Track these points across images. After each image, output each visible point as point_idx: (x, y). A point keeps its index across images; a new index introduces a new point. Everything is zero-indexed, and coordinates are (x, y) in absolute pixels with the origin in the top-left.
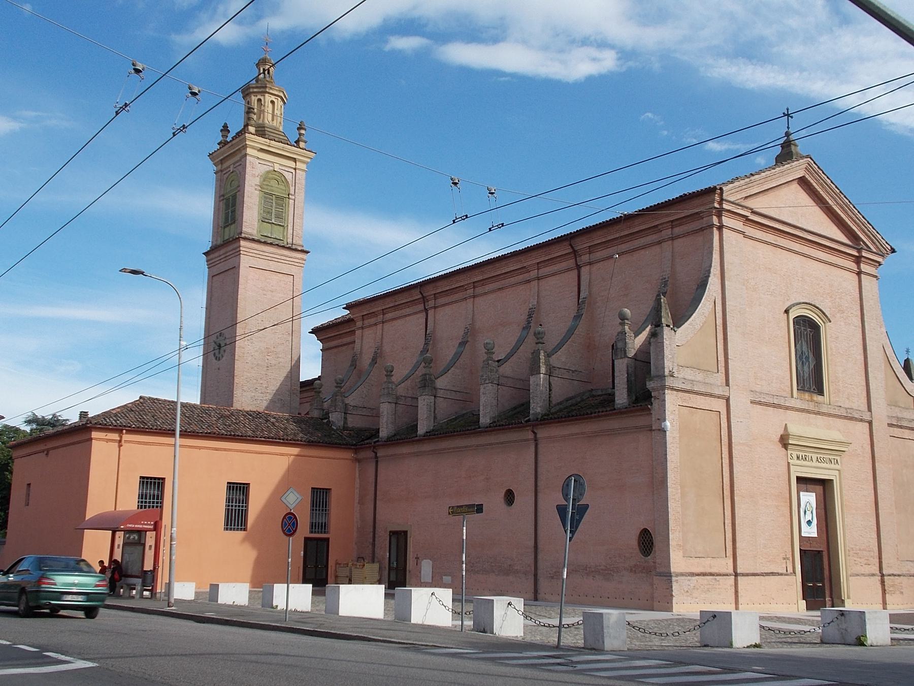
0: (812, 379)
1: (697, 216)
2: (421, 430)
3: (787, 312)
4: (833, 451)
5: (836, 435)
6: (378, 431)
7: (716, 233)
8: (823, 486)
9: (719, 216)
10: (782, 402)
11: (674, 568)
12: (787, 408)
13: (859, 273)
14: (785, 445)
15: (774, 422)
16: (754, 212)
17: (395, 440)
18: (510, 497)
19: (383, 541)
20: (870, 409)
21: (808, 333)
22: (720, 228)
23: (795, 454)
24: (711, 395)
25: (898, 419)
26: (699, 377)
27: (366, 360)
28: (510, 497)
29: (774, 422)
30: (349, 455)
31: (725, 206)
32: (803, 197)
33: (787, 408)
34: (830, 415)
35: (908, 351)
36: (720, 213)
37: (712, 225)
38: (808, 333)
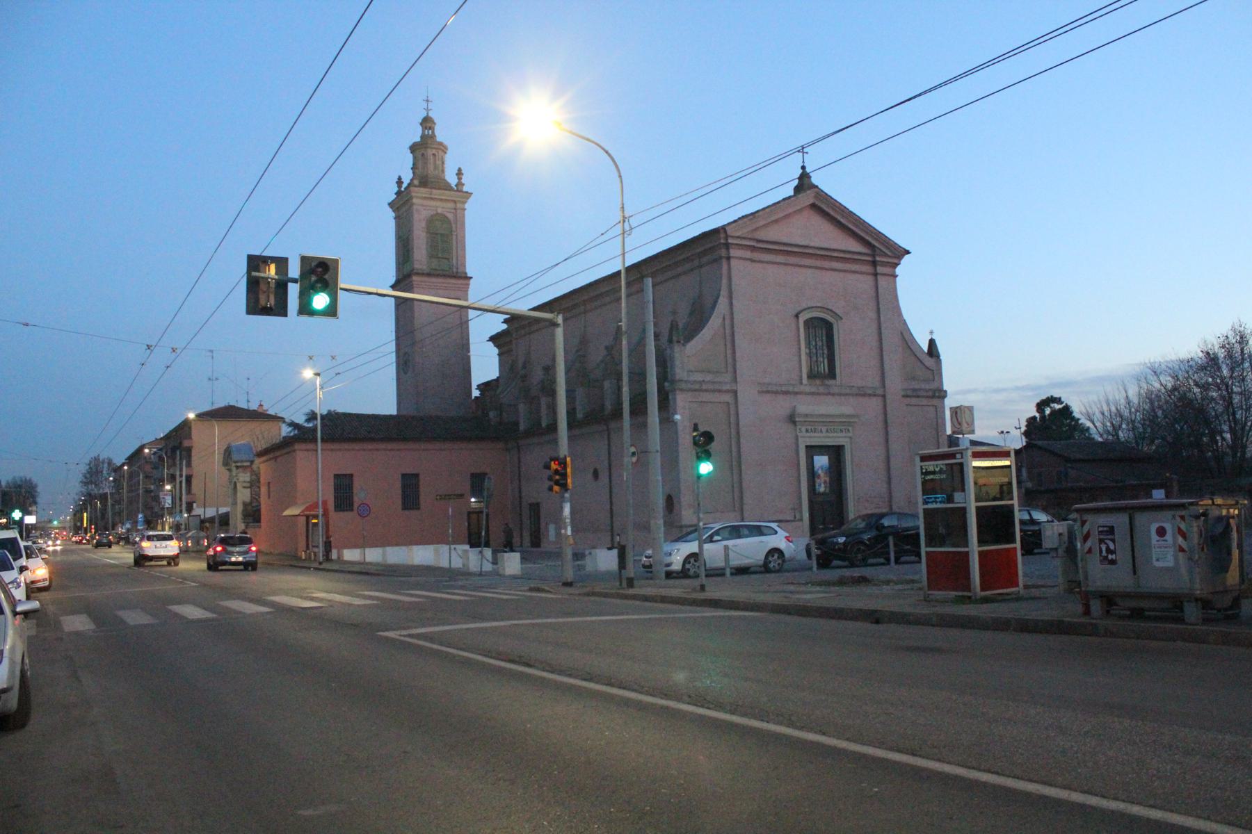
0: (824, 370)
1: (712, 249)
2: (544, 424)
3: (797, 316)
4: (846, 423)
5: (847, 410)
6: (517, 424)
7: (724, 262)
8: (836, 452)
9: (728, 249)
10: (791, 389)
11: (367, 550)
12: (796, 393)
13: (876, 274)
14: (794, 423)
15: (782, 406)
16: (759, 241)
17: (528, 434)
18: (596, 474)
19: (526, 512)
20: (884, 386)
21: (822, 331)
22: (728, 258)
23: (804, 429)
24: (720, 391)
25: (914, 390)
26: (709, 378)
27: (520, 364)
28: (596, 474)
29: (782, 406)
30: (501, 445)
31: (730, 241)
32: (816, 220)
33: (796, 393)
34: (840, 395)
35: (931, 332)
36: (727, 246)
37: (721, 258)
38: (822, 331)
